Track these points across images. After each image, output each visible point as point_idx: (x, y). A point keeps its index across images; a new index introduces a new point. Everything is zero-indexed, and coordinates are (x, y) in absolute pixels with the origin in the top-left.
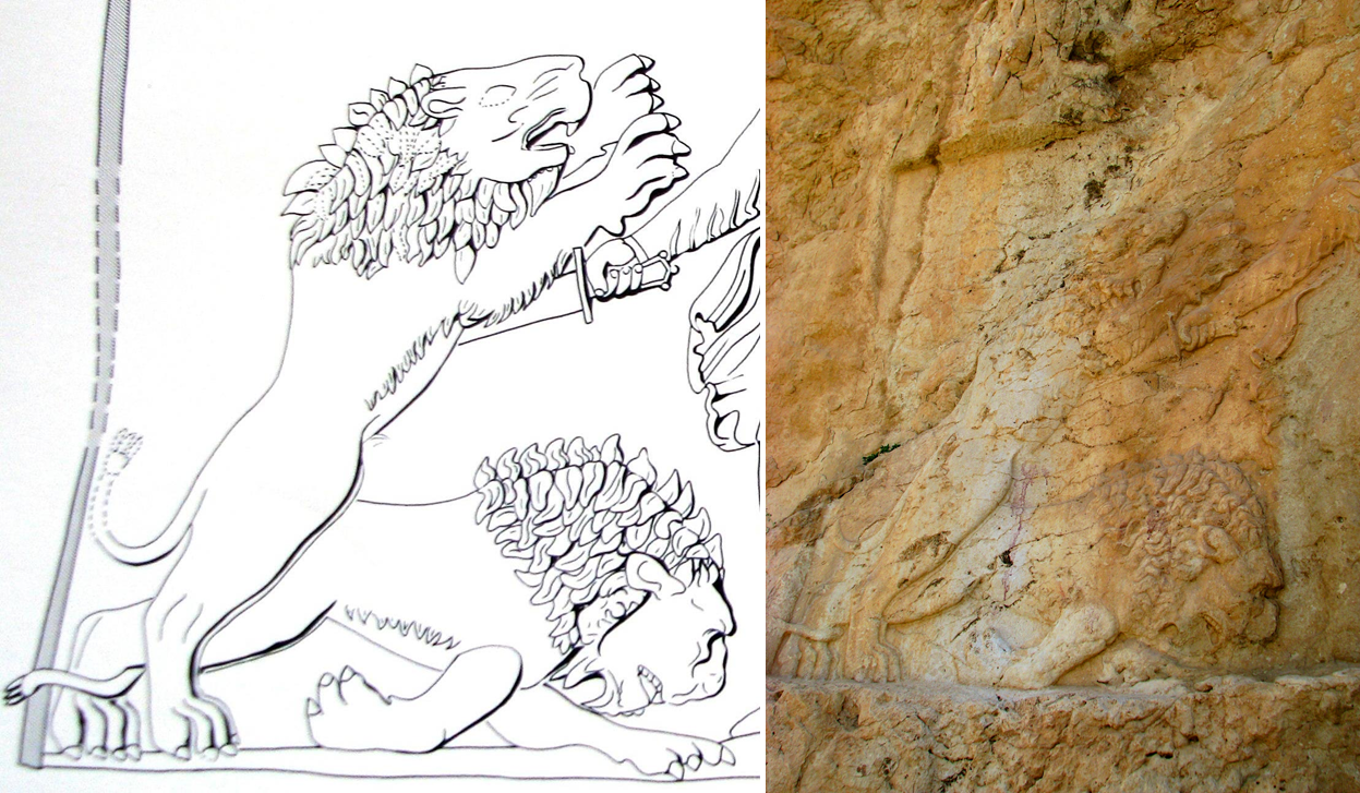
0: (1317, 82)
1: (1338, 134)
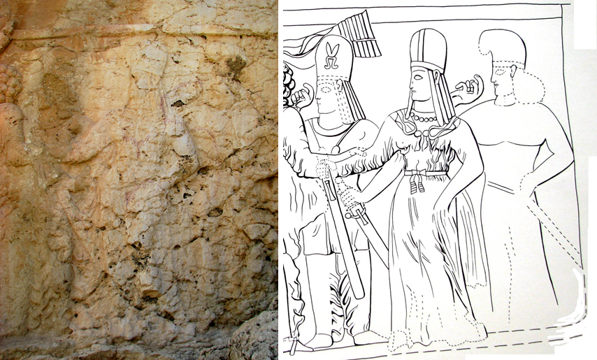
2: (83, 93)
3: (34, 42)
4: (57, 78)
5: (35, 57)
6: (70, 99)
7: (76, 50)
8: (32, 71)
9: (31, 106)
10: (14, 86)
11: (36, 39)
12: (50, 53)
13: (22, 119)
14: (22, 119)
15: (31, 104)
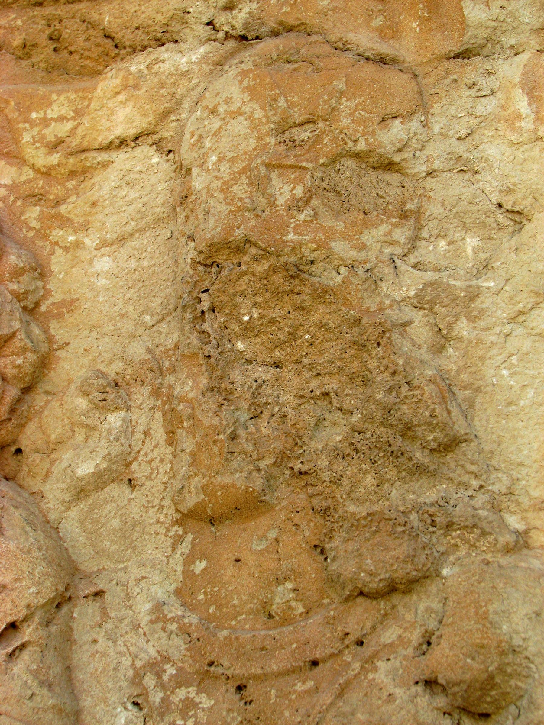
2: (499, 374)
4: (297, 272)
5: (122, 117)
6: (407, 430)
7: (407, 49)
8: (112, 223)
9: (117, 491)
12: (230, 87)
13: (61, 601)
14: (61, 601)
15: (120, 472)
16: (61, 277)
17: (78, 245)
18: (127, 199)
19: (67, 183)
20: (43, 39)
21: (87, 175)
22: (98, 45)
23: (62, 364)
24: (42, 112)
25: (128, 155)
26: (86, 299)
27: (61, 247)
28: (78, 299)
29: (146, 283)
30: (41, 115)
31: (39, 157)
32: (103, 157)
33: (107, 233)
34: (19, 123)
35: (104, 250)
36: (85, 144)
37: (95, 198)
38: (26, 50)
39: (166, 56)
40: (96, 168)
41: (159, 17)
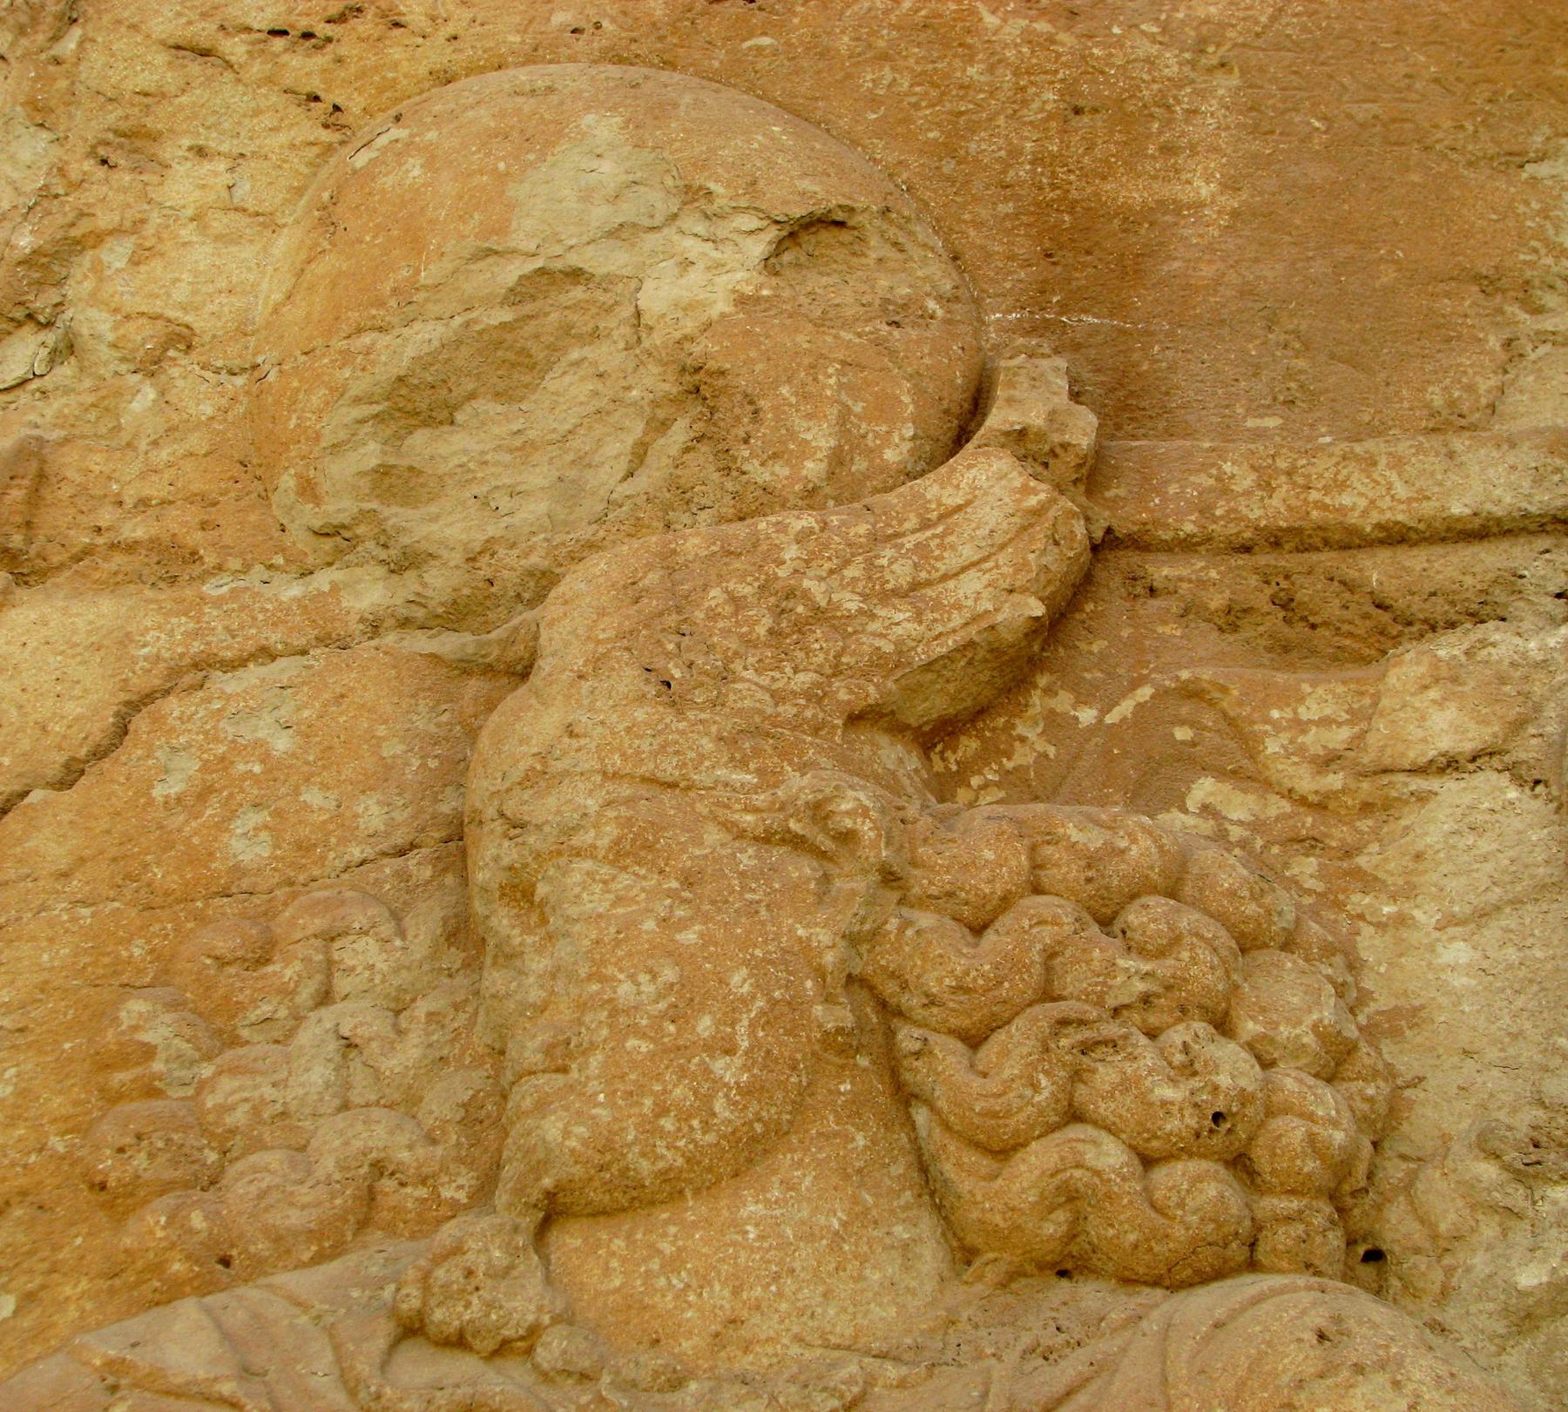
0: (70, 776)
1: (151, 1091)
3: (1375, 570)
5: (1445, 727)
10: (1334, 1062)
11: (1396, 537)
16: (1382, 970)
17: (1401, 920)
18: (1475, 851)
19: (1358, 824)
20: (1262, 601)
21: (1392, 812)
22: (1366, 616)
23: (1419, 1110)
24: (1288, 710)
25: (1463, 784)
26: (1440, 1007)
27: (1370, 923)
28: (1423, 1007)
29: (1546, 985)
30: (1288, 714)
31: (1301, 778)
32: (1417, 783)
33: (1452, 902)
34: (1254, 723)
35: (1452, 931)
36: (1387, 761)
37: (1420, 846)
38: (1231, 618)
39: (1496, 637)
40: (1406, 802)
41: (1468, 581)
